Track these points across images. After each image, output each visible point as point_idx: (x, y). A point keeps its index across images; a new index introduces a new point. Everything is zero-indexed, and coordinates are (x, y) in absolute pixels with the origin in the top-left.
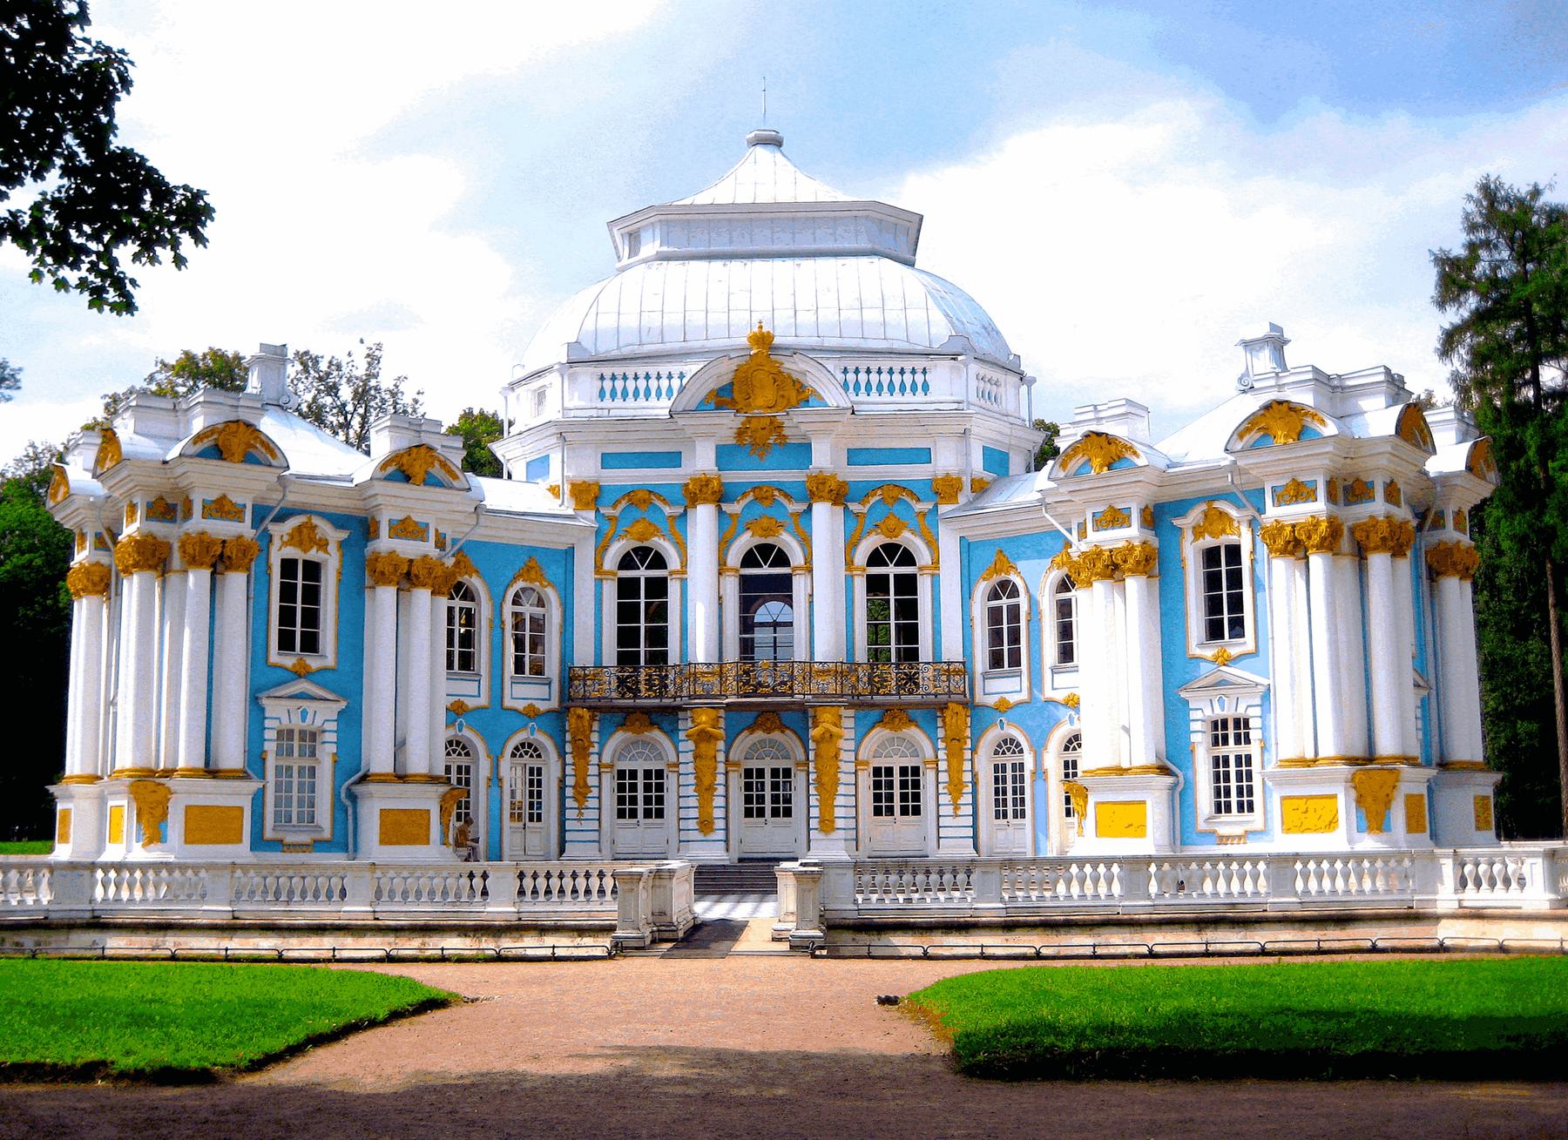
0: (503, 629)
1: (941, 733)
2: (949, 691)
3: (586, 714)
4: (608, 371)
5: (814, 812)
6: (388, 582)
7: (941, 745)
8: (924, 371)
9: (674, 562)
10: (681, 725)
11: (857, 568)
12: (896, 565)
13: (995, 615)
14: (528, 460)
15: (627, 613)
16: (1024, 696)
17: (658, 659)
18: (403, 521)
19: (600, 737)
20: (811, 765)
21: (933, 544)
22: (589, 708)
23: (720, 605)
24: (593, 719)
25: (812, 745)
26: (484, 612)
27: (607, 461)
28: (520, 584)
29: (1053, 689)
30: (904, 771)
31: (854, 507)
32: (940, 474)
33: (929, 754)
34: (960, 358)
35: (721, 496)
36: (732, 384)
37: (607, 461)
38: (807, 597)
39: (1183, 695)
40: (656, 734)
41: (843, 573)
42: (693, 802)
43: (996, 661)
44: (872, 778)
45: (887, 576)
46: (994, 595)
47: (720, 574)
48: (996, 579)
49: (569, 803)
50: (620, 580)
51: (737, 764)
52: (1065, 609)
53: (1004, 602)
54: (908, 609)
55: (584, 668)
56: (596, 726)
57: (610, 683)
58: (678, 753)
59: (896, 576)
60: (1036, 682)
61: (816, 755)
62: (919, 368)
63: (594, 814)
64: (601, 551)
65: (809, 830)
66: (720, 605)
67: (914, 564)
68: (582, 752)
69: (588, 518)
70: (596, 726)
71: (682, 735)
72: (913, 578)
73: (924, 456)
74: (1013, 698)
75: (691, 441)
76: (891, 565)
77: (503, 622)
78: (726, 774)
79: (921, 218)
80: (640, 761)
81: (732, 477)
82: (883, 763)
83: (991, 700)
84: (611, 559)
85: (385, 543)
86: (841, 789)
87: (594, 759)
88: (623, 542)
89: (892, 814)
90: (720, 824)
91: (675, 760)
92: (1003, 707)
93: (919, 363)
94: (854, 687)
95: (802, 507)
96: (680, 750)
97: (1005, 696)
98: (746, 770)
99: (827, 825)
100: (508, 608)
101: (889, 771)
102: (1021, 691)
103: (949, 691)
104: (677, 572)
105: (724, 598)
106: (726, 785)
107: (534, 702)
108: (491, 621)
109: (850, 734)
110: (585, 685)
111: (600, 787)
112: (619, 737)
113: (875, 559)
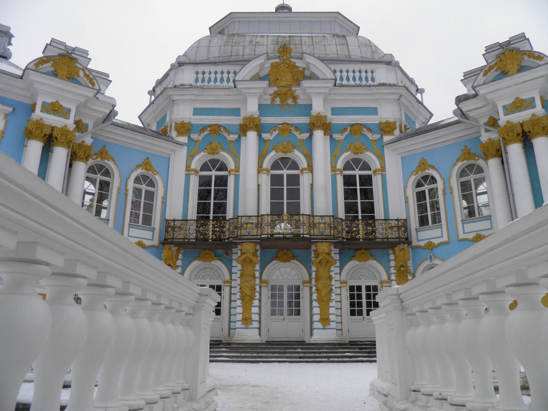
0: (126, 194)
1: (393, 263)
2: (399, 236)
3: (174, 248)
4: (200, 68)
5: (316, 310)
6: (36, 138)
7: (392, 270)
8: (372, 72)
9: (231, 165)
10: (234, 257)
11: (338, 170)
12: (360, 170)
13: (421, 196)
14: (157, 120)
15: (203, 195)
16: (445, 239)
17: (220, 219)
18: (52, 104)
19: (183, 263)
20: (313, 281)
21: (381, 157)
22: (176, 244)
23: (259, 189)
24: (178, 251)
25: (314, 268)
26: (116, 183)
27: (197, 112)
28: (140, 171)
29: (464, 233)
30: (368, 288)
31: (336, 136)
32: (384, 121)
33: (385, 277)
34: (392, 63)
35: (259, 128)
36: (269, 74)
37: (197, 112)
38: (310, 185)
40: (218, 263)
41: (329, 173)
42: (239, 303)
43: (423, 221)
44: (349, 293)
45: (355, 176)
46: (419, 185)
47: (259, 172)
48: (421, 174)
50: (201, 177)
51: (267, 282)
52: (465, 187)
53: (426, 188)
54: (368, 194)
55: (174, 221)
56: (180, 256)
57: (189, 230)
58: (231, 273)
59: (360, 176)
60: (452, 230)
61: (316, 275)
62: (369, 70)
64: (190, 157)
65: (312, 322)
66: (259, 189)
67: (370, 169)
69: (184, 139)
70: (180, 256)
71: (234, 263)
72: (370, 178)
73: (374, 111)
74: (436, 241)
75: (245, 101)
76: (357, 170)
77: (127, 190)
78: (260, 287)
79: (359, 28)
80: (208, 279)
81: (267, 120)
82: (355, 283)
83: (422, 244)
84: (196, 164)
85: (38, 114)
86: (333, 296)
88: (202, 154)
89: (362, 315)
90: (255, 317)
91: (227, 277)
92: (430, 246)
93: (369, 67)
94: (339, 232)
95: (307, 135)
96: (233, 271)
97: (431, 240)
98: (272, 287)
99: (325, 321)
100: (131, 185)
101: (359, 288)
102: (442, 237)
103: (399, 236)
104: (233, 170)
105: (261, 186)
106: (260, 294)
107: (142, 240)
108: (119, 189)
109: (338, 264)
110: (174, 231)
112: (196, 263)
113: (347, 166)
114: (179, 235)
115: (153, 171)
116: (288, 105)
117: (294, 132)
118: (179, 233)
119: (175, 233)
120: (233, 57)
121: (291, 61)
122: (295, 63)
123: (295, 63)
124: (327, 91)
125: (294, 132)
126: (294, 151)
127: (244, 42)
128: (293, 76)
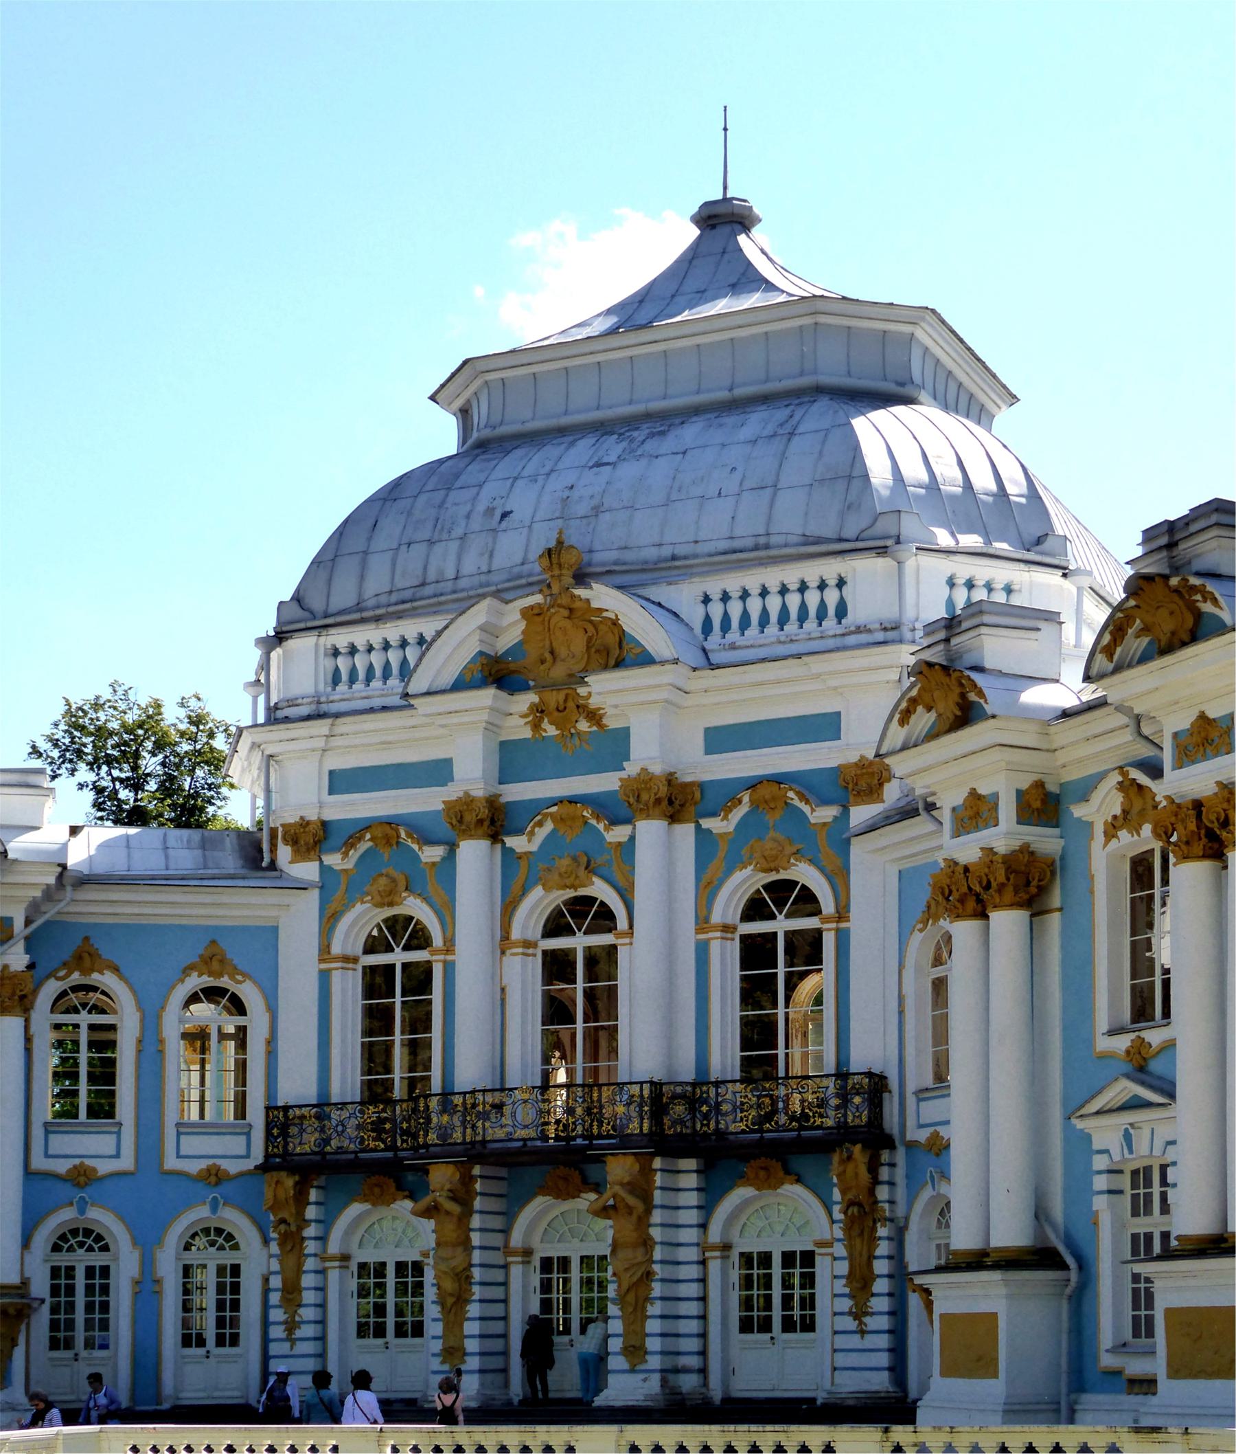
39: (1079, 1124)
49: (277, 1315)
63: (307, 1331)
68: (292, 1241)
70: (313, 1195)
87: (311, 1247)
111: (322, 1289)
112: (356, 1209)
114: (305, 1143)
115: (234, 971)
116: (579, 733)
117: (593, 822)
118: (298, 1140)
119: (289, 1139)
120: (428, 590)
121: (573, 596)
122: (588, 601)
123: (588, 601)
124: (664, 694)
125: (593, 822)
126: (593, 884)
127: (468, 516)
128: (590, 639)
